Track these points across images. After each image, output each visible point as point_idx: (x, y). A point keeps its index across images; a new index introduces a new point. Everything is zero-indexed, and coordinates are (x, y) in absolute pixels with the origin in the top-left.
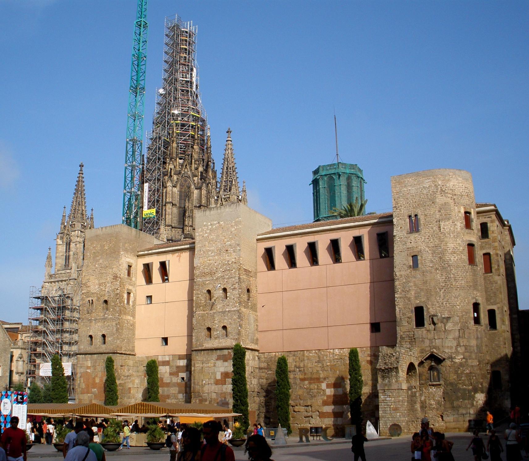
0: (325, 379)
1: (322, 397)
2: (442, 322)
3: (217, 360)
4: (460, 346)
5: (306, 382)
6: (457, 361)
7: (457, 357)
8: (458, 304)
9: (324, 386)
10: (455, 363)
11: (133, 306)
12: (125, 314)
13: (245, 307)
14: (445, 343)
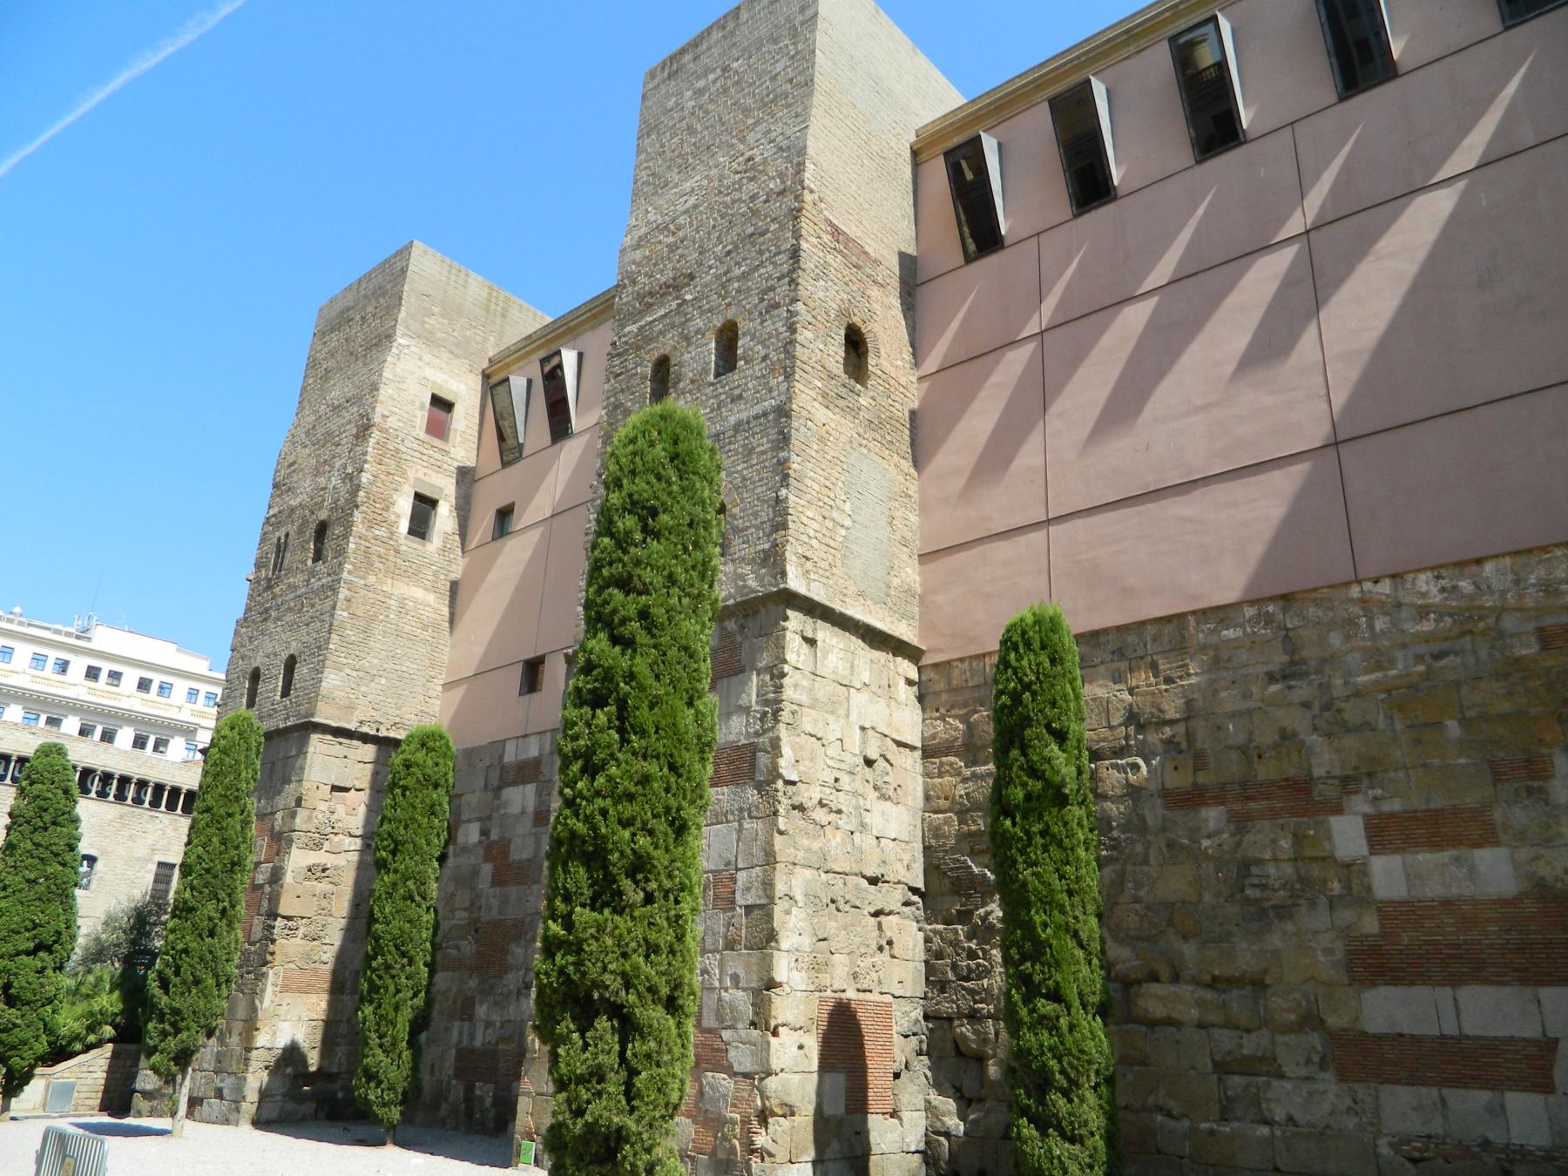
0: (1348, 783)
1: (1346, 916)
5: (1213, 816)
9: (1347, 834)
12: (395, 574)
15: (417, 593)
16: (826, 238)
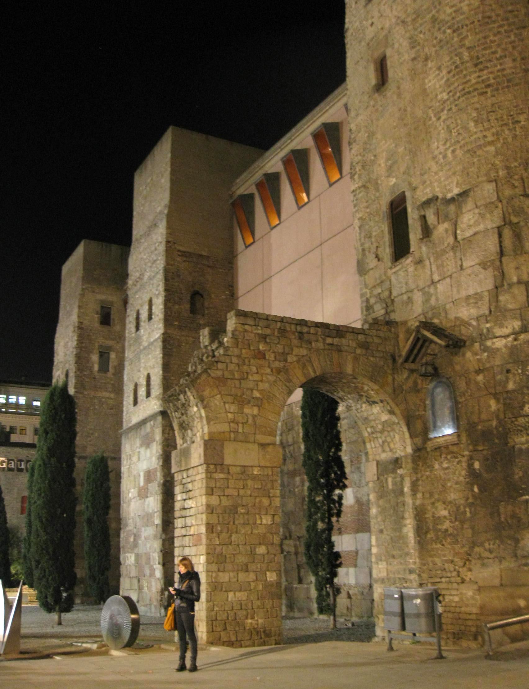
2: (447, 218)
3: (141, 446)
4: (510, 285)
6: (499, 343)
7: (498, 332)
8: (490, 138)
10: (493, 352)
11: (113, 374)
13: (180, 328)
14: (459, 286)
15: (106, 394)
16: (179, 259)
